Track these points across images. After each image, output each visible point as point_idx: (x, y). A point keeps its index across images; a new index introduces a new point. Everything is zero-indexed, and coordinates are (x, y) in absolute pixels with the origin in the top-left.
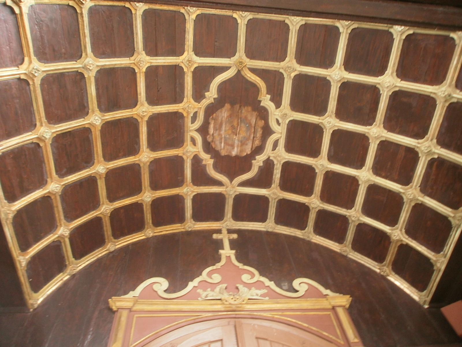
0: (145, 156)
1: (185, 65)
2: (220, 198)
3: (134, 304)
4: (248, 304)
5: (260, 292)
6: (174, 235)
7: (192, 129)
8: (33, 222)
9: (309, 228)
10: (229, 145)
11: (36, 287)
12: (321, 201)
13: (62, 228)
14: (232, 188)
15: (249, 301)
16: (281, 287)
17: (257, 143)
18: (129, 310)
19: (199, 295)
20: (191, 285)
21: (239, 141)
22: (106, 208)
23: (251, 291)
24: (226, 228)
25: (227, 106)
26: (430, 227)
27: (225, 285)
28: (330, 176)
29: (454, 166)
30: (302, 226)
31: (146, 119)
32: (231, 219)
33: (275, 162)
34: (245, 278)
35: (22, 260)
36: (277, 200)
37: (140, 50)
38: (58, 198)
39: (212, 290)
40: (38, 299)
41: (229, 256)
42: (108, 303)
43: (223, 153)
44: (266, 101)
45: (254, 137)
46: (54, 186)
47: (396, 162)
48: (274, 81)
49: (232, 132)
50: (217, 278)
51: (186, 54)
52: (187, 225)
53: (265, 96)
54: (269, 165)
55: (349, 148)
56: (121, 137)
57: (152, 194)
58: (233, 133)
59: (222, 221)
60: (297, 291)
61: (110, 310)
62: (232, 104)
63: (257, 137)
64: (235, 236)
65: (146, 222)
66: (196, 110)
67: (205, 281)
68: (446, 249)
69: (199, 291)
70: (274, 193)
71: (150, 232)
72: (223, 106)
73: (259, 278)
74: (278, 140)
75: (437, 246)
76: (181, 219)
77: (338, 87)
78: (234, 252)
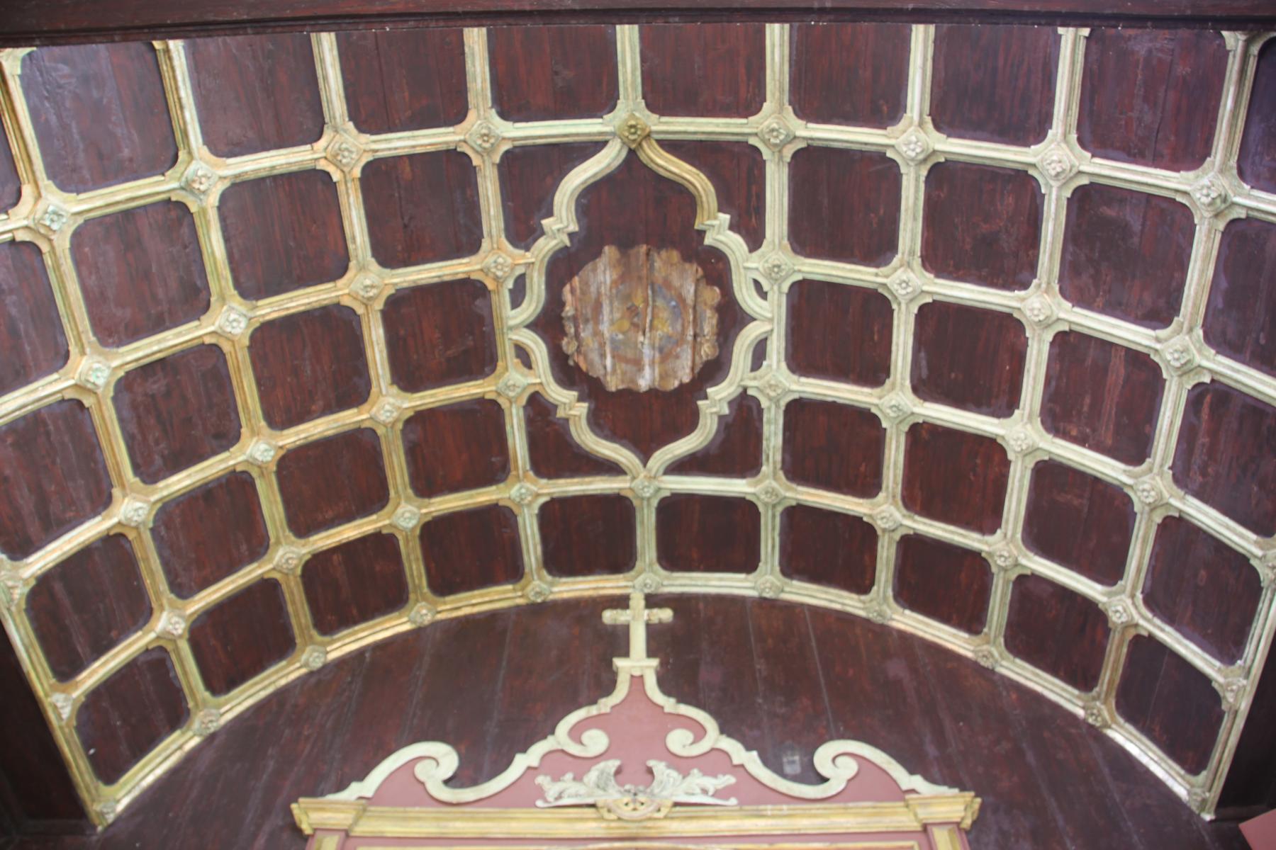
0: (388, 406)
1: (473, 148)
2: (617, 511)
3: (356, 821)
4: (672, 818)
5: (712, 783)
6: (493, 616)
7: (515, 322)
8: (85, 604)
10: (627, 361)
11: (110, 771)
12: (905, 512)
13: (165, 615)
14: (648, 480)
15: (678, 809)
16: (779, 771)
17: (707, 350)
18: (343, 834)
19: (540, 793)
20: (521, 763)
21: (653, 348)
22: (286, 555)
23: (689, 779)
24: (639, 593)
25: (609, 252)
26: (1204, 586)
27: (613, 764)
28: (924, 438)
29: (1256, 409)
30: (861, 583)
31: (379, 305)
32: (657, 567)
33: (765, 403)
34: (678, 741)
35: (62, 703)
36: (780, 509)
37: (338, 120)
38: (147, 537)
39: (578, 778)
40: (113, 800)
41: (642, 677)
42: (290, 813)
43: (613, 384)
44: (718, 230)
45: (695, 336)
46: (133, 508)
47: (1103, 393)
48: (736, 171)
50: (596, 741)
51: (472, 115)
52: (529, 588)
53: (716, 218)
54: (746, 411)
55: (969, 356)
56: (311, 361)
57: (420, 508)
58: (635, 325)
59: (633, 573)
60: (824, 780)
61: (296, 830)
62: (625, 245)
64: (666, 615)
65: (411, 586)
67: (563, 751)
68: (1249, 650)
69: (542, 780)
70: (768, 488)
71: (424, 611)
72: (598, 254)
73: (717, 741)
74: (766, 339)
75: (1228, 645)
76: (514, 572)
77: (923, 179)
78: (655, 662)
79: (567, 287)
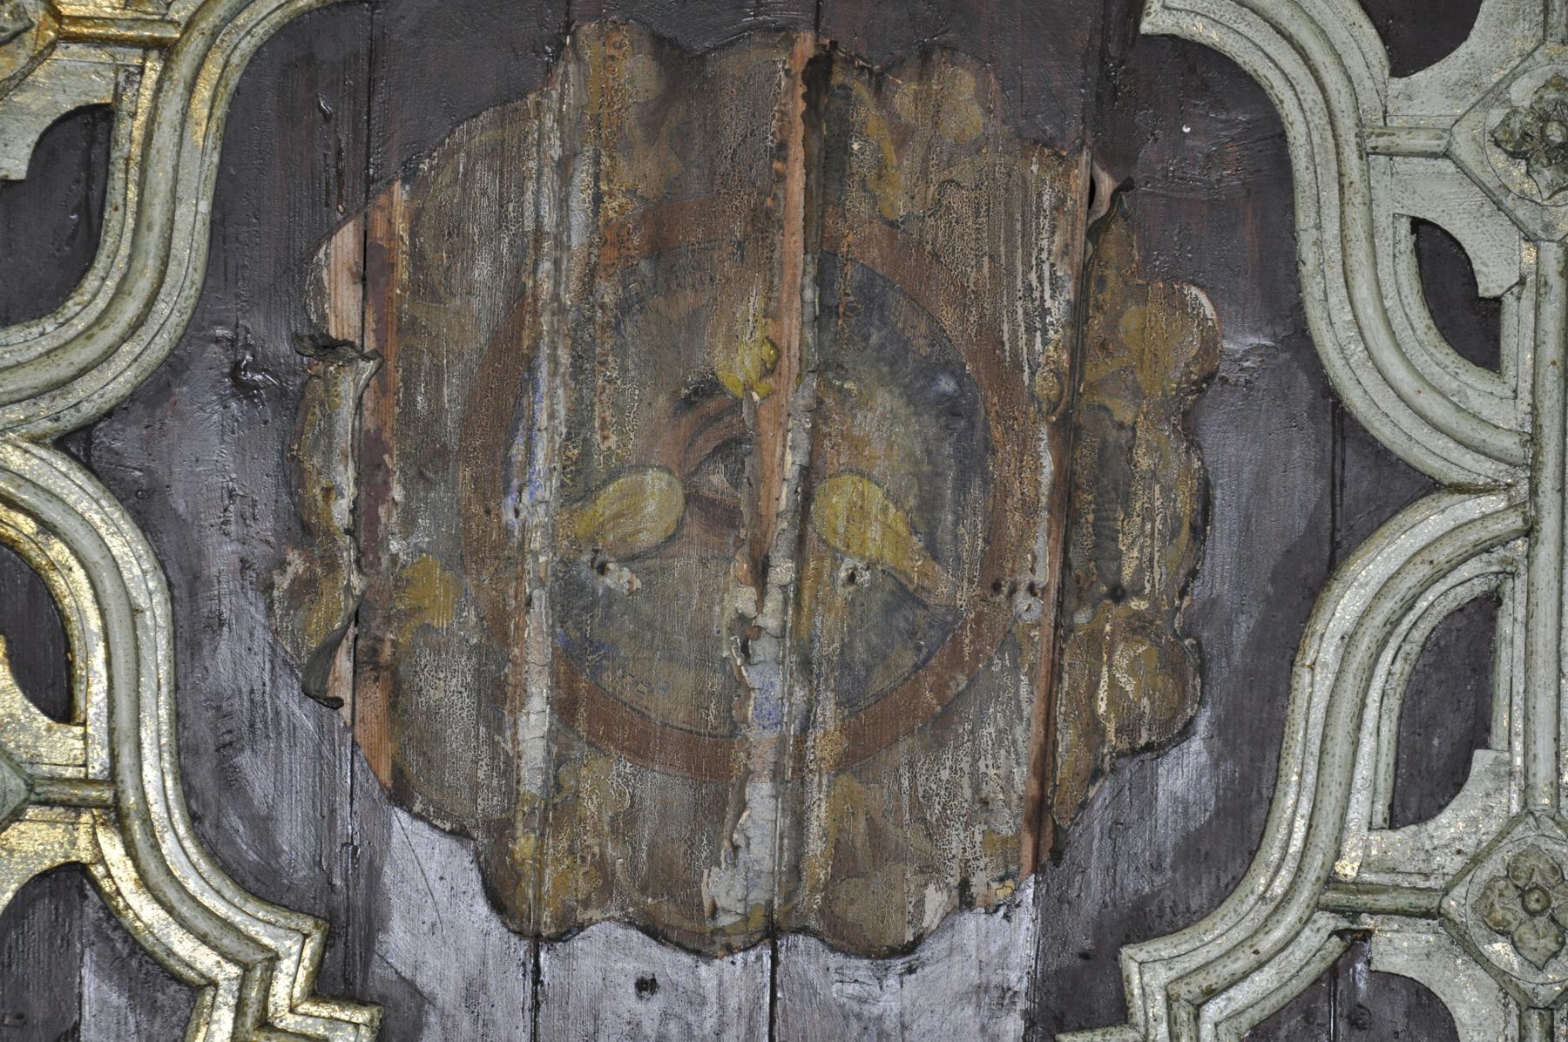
45: (1070, 592)
58: (717, 516)
63: (1118, 594)
74: (1488, 605)
79: (345, 242)
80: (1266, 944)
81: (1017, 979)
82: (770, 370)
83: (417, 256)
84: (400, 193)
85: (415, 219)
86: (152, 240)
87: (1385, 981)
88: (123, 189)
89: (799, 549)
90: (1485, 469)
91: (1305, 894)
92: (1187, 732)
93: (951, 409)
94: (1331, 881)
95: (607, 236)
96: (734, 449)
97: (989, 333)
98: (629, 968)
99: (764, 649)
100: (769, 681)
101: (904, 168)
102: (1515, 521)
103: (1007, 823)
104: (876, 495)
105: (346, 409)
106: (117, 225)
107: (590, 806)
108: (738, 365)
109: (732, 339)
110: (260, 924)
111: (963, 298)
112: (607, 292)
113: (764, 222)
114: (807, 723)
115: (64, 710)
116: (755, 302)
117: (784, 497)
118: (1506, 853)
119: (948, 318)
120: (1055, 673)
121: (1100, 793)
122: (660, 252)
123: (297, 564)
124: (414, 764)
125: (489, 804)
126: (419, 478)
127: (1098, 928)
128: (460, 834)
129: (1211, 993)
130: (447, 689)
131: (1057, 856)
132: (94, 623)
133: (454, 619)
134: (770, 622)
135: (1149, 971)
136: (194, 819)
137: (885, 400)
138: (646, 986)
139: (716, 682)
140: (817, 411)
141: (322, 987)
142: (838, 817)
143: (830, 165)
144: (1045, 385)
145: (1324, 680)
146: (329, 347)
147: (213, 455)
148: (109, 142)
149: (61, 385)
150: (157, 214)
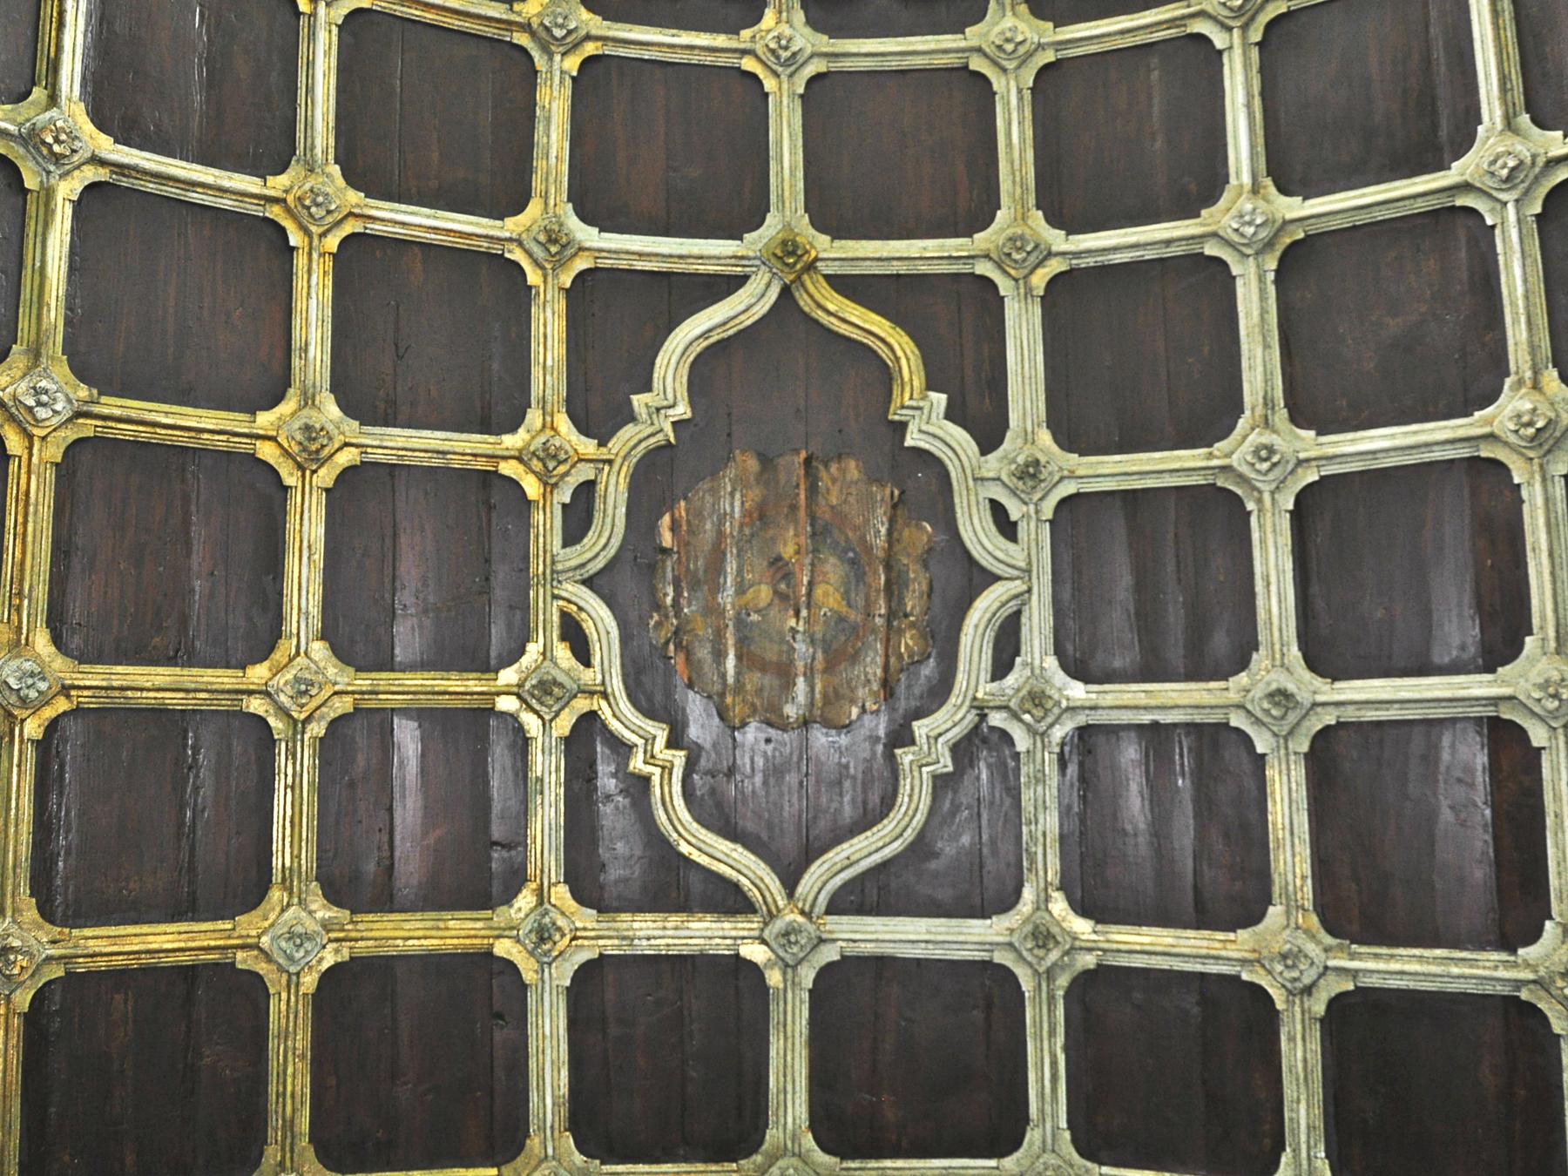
1: (529, 254)
9: (1296, 1151)
10: (764, 667)
12: (1329, 940)
21: (813, 642)
36: (1063, 981)
44: (929, 423)
45: (891, 616)
49: (776, 592)
53: (924, 398)
63: (906, 616)
66: (585, 473)
74: (1017, 614)
77: (1271, 276)
79: (667, 519)
80: (957, 718)
81: (882, 733)
82: (797, 552)
83: (688, 522)
84: (683, 503)
85: (687, 511)
86: (609, 520)
87: (993, 729)
88: (598, 504)
89: (809, 607)
90: (1016, 573)
91: (967, 703)
92: (929, 656)
93: (853, 562)
94: (975, 699)
95: (746, 513)
96: (788, 576)
97: (863, 539)
98: (762, 736)
99: (799, 637)
100: (801, 647)
101: (835, 490)
102: (1025, 587)
103: (875, 687)
104: (831, 589)
105: (669, 569)
106: (598, 517)
107: (749, 687)
108: (788, 551)
109: (785, 545)
110: (651, 727)
111: (856, 528)
112: (747, 531)
113: (794, 508)
114: (813, 659)
115: (587, 664)
116: (791, 533)
117: (804, 591)
118: (1027, 688)
119: (850, 534)
120: (888, 640)
121: (903, 677)
122: (761, 517)
123: (656, 617)
124: (694, 676)
125: (717, 687)
126: (692, 589)
127: (905, 717)
128: (709, 697)
129: (940, 735)
130: (704, 653)
131: (892, 695)
132: (595, 637)
133: (704, 631)
134: (801, 628)
135: (921, 728)
136: (629, 696)
137: (832, 560)
138: (768, 741)
139: (785, 648)
140: (812, 564)
141: (672, 744)
142: (824, 687)
143: (813, 490)
144: (881, 554)
145: (970, 638)
146: (665, 551)
147: (628, 585)
148: (594, 492)
149: (583, 565)
150: (610, 511)
